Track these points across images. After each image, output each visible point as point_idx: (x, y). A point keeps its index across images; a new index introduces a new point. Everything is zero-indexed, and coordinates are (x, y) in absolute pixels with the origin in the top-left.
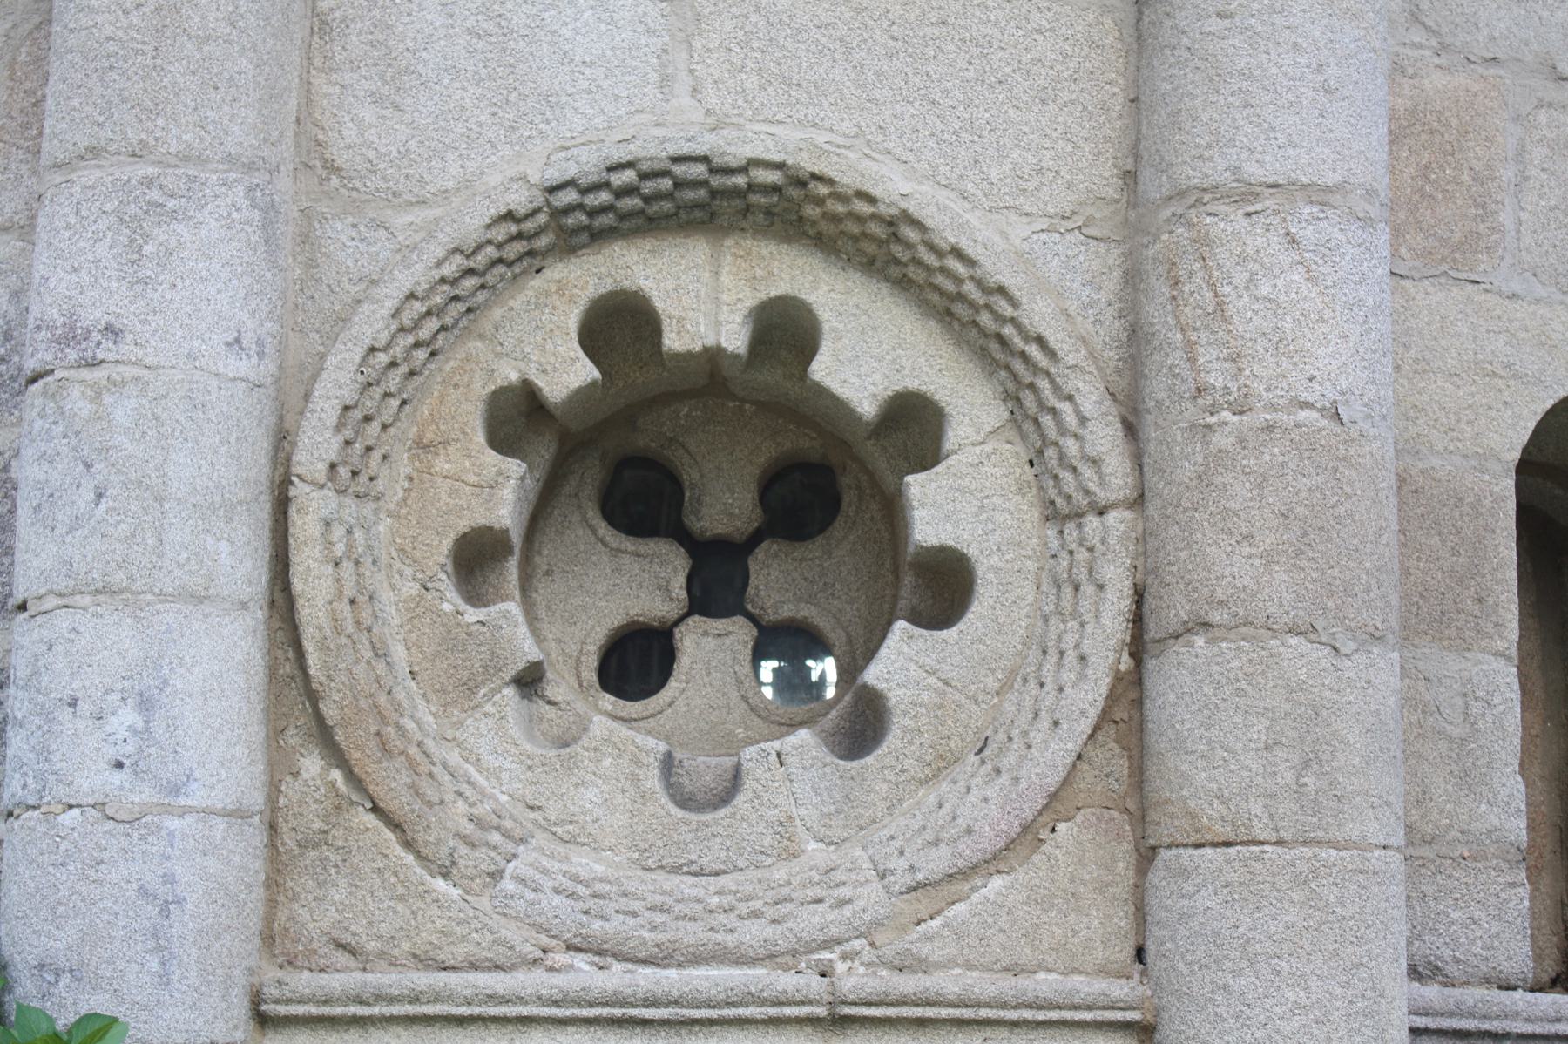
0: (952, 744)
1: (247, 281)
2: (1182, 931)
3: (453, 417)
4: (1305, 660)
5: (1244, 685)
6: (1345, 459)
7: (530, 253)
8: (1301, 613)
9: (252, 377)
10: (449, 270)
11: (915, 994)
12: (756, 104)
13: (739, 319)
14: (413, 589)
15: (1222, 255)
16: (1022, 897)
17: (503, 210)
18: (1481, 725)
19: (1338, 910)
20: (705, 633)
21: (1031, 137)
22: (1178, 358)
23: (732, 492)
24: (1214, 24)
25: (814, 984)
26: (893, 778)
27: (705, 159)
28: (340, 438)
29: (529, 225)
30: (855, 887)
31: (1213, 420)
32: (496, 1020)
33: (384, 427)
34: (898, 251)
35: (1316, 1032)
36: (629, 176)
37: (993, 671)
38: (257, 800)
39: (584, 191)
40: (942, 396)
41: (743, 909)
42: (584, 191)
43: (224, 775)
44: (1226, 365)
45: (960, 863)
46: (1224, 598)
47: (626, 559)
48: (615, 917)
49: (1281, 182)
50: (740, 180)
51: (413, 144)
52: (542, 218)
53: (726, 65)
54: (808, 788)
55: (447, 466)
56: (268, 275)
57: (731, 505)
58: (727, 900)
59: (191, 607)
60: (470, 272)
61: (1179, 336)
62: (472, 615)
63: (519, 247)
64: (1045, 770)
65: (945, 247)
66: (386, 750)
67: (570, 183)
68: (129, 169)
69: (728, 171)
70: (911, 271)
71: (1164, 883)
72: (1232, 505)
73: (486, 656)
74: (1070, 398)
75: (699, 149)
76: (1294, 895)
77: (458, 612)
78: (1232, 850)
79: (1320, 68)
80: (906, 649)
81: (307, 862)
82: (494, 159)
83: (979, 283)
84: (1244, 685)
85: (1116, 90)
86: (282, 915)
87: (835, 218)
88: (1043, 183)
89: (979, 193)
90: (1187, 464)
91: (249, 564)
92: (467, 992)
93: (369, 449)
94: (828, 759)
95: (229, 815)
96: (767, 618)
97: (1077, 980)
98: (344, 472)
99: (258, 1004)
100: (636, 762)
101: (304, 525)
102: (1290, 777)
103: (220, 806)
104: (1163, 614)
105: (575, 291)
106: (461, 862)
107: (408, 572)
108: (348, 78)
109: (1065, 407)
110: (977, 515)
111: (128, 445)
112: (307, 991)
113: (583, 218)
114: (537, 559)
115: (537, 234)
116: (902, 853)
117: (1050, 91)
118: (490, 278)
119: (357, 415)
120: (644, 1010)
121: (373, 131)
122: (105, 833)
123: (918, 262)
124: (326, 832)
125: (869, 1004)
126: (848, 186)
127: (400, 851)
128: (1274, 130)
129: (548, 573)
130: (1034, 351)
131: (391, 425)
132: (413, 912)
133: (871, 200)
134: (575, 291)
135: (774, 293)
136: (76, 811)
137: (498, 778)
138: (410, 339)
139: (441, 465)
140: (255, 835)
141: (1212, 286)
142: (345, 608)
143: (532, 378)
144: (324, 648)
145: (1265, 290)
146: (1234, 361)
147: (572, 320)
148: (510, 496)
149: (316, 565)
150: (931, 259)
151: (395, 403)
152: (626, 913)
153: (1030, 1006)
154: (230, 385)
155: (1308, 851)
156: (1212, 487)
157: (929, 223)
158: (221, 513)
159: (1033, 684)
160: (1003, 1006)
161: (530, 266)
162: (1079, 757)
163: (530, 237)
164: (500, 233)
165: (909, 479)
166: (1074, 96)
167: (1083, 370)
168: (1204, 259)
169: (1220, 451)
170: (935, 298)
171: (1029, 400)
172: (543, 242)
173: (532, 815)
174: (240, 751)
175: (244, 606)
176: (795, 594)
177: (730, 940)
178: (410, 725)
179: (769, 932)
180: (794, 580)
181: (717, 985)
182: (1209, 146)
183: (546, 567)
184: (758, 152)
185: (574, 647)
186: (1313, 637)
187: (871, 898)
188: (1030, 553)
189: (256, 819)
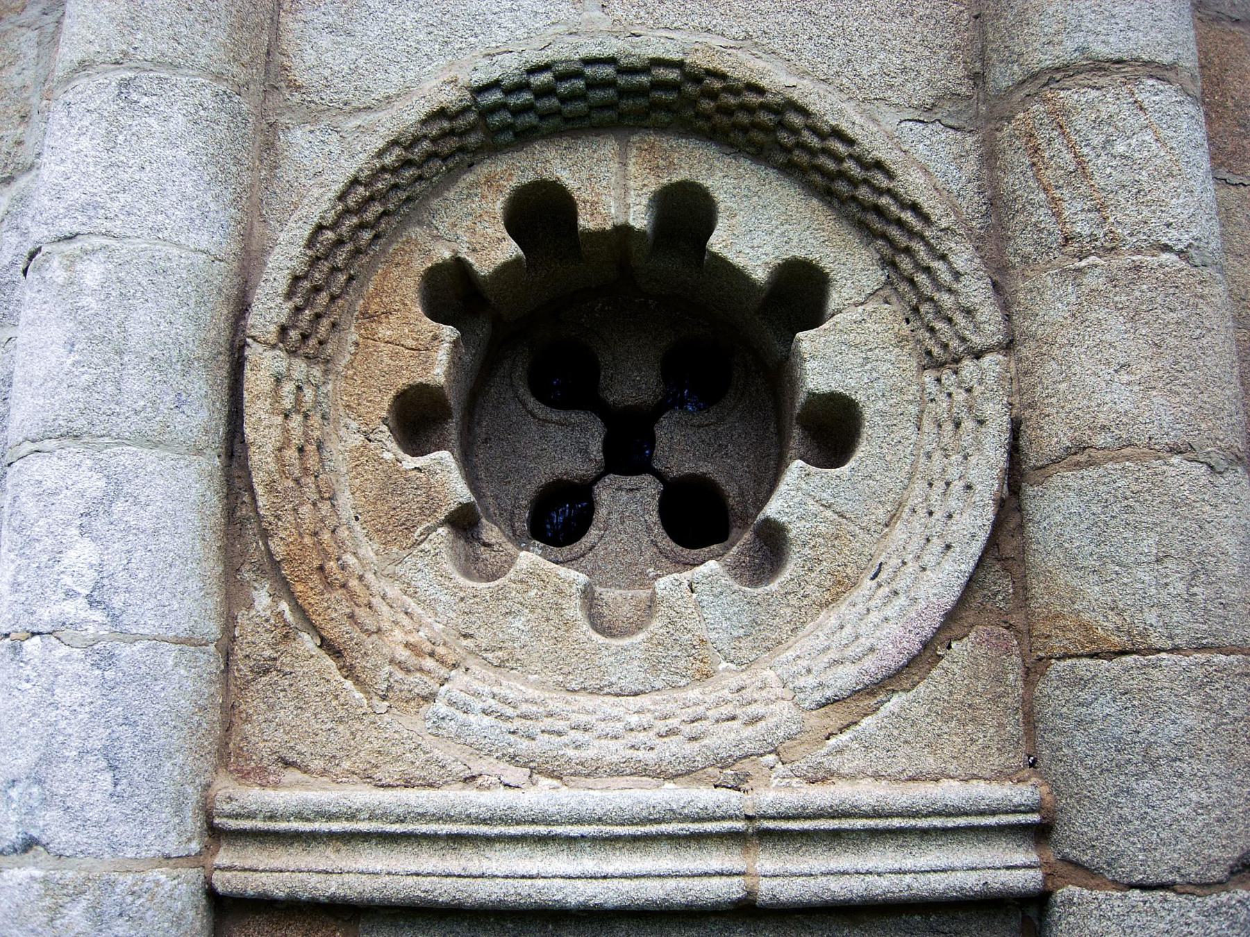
0: (849, 570)
2: (1079, 736)
3: (395, 291)
4: (1186, 478)
5: (1131, 502)
6: (1202, 297)
7: (462, 149)
8: (1179, 433)
9: (214, 251)
10: (389, 160)
11: (831, 807)
12: (656, 15)
13: (645, 201)
14: (359, 440)
15: (1080, 122)
16: (923, 710)
17: (436, 107)
19: (1231, 712)
20: (620, 489)
21: (894, 42)
22: (1043, 216)
23: (640, 370)
25: (733, 800)
26: (795, 602)
27: (611, 61)
28: (290, 305)
29: (461, 123)
30: (767, 704)
32: (425, 836)
33: (333, 298)
34: (784, 137)
35: (1218, 830)
36: (546, 77)
37: (883, 503)
38: (213, 629)
40: (827, 264)
41: (661, 726)
42: (509, 91)
43: (176, 606)
44: (1091, 215)
45: (867, 680)
46: (1106, 423)
47: (552, 428)
48: (540, 737)
49: (1125, 58)
50: (644, 79)
51: (362, 61)
52: (472, 117)
54: (718, 614)
55: (388, 333)
56: (234, 169)
57: (639, 381)
58: (646, 719)
59: (146, 451)
60: (407, 163)
61: (1042, 196)
62: (410, 462)
63: (453, 143)
64: (942, 590)
65: (826, 128)
66: (329, 585)
67: (495, 85)
68: (111, 75)
69: (632, 71)
71: (1058, 692)
72: (1107, 337)
73: (423, 499)
74: (943, 257)
75: (608, 52)
76: (1191, 699)
77: (397, 460)
78: (1129, 660)
80: (804, 486)
81: (259, 687)
82: (430, 68)
83: (859, 160)
85: (962, 8)
86: (235, 739)
87: (727, 111)
88: (907, 80)
89: (852, 86)
90: (1060, 305)
92: (400, 811)
93: (318, 316)
94: (736, 587)
95: (181, 643)
96: (671, 475)
98: (294, 334)
100: (559, 592)
101: (257, 381)
102: (1181, 587)
104: (1044, 442)
105: (501, 182)
106: (397, 686)
107: (354, 425)
108: (311, 15)
109: (937, 265)
110: (862, 365)
111: (93, 305)
112: (254, 807)
113: (507, 117)
114: (477, 430)
116: (809, 671)
117: (907, 7)
119: (306, 284)
120: (569, 827)
121: (329, 54)
122: (61, 659)
123: (803, 146)
124: (275, 659)
125: (788, 818)
126: (738, 80)
128: (1114, 16)
129: (486, 441)
130: (907, 216)
131: (339, 297)
132: (352, 733)
133: (760, 91)
134: (501, 182)
135: (675, 179)
136: (37, 639)
137: (434, 609)
139: (384, 332)
140: (209, 661)
141: (1072, 148)
142: (291, 454)
143: (463, 256)
144: (271, 488)
145: (1121, 148)
146: (1098, 210)
147: (498, 205)
148: (444, 357)
149: (267, 416)
150: (814, 141)
151: (342, 278)
152: (550, 733)
153: (938, 814)
154: (192, 255)
155: (1201, 657)
156: (1087, 323)
157: (812, 108)
158: (179, 367)
159: (922, 513)
160: (916, 814)
161: (462, 160)
162: (971, 579)
163: (463, 134)
164: (434, 130)
165: (800, 335)
166: (928, 12)
167: (954, 233)
168: (1061, 127)
169: (1092, 290)
170: (817, 178)
171: (905, 263)
172: (473, 139)
173: (465, 642)
174: (193, 584)
175: (200, 452)
176: (694, 455)
177: (650, 757)
178: (349, 559)
179: (691, 748)
180: (693, 443)
181: (640, 802)
182: (1058, 33)
183: (484, 436)
184: (660, 53)
185: (509, 502)
186: (1192, 456)
187: (781, 715)
188: (911, 398)
189: (212, 648)
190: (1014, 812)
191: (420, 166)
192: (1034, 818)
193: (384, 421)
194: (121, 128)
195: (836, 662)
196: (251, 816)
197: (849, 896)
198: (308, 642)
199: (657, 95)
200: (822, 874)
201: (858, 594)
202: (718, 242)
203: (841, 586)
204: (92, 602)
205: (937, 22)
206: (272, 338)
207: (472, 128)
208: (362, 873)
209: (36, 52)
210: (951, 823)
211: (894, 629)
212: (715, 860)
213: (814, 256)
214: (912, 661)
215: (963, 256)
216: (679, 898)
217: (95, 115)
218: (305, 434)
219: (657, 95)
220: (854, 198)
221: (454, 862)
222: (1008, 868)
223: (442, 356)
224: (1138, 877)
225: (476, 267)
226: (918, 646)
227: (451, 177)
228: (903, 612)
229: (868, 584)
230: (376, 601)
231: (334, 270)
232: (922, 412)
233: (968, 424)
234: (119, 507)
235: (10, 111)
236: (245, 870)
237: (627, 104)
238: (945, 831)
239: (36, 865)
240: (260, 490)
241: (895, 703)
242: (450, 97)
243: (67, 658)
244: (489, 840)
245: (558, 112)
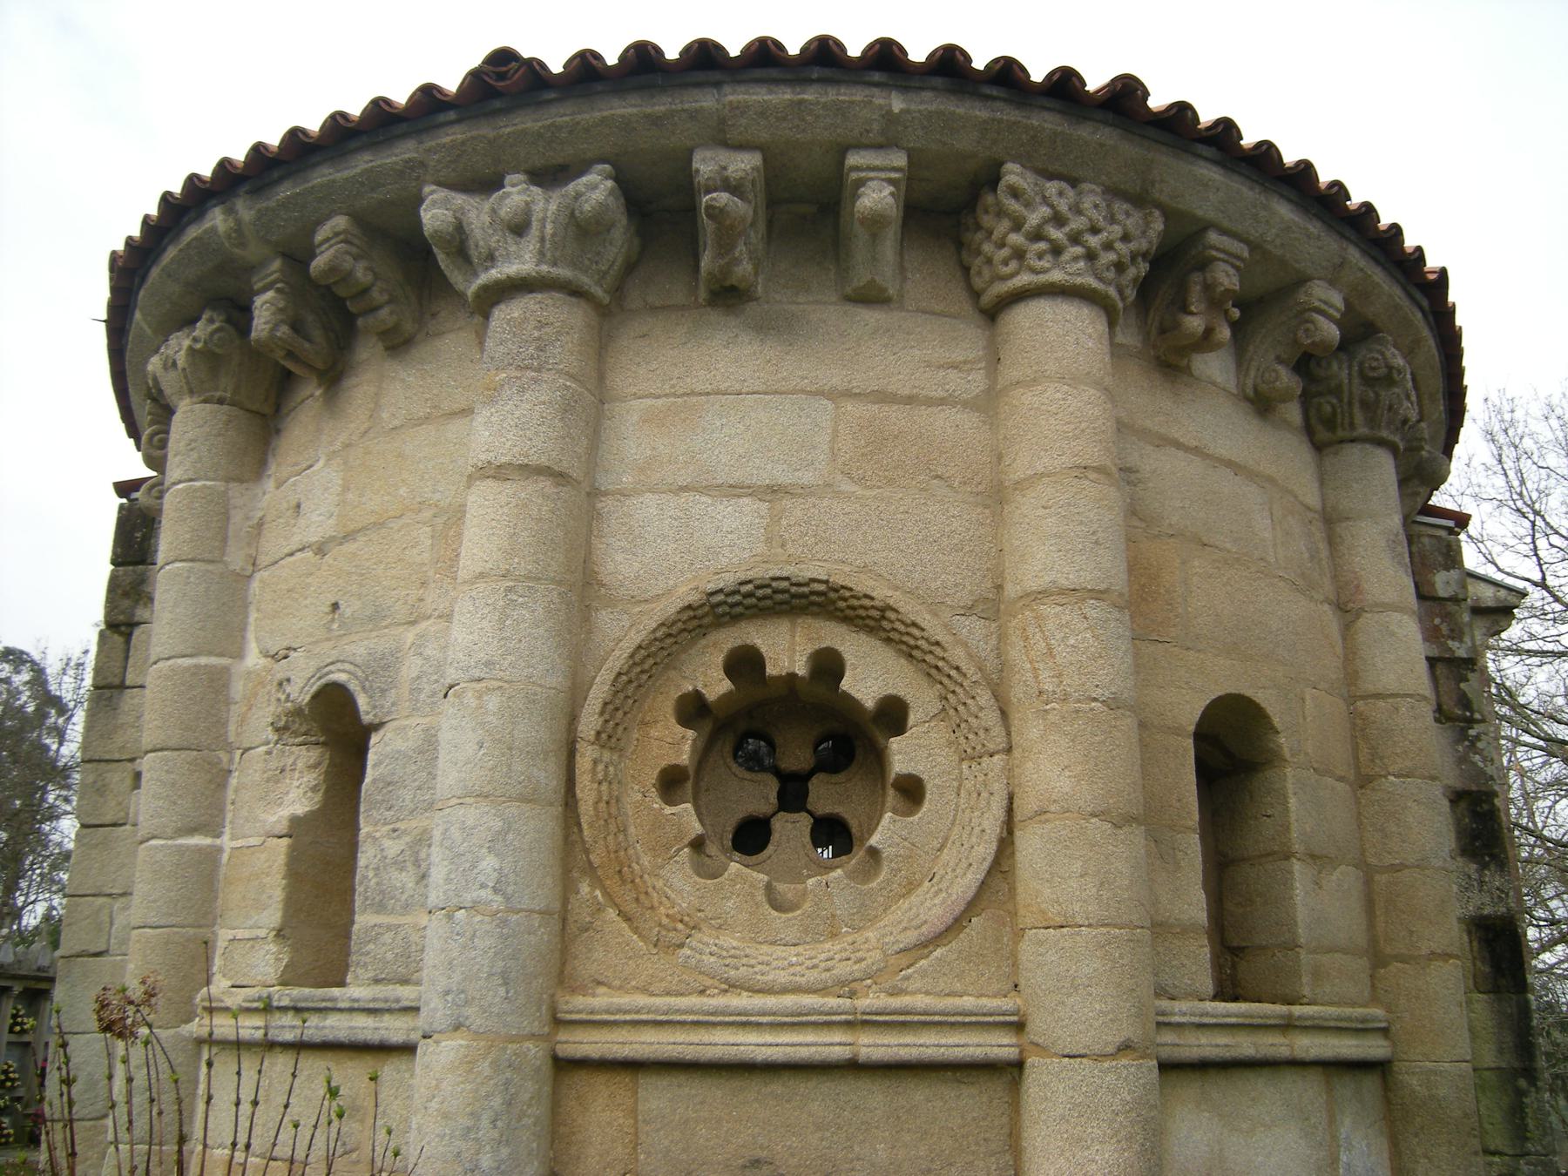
1: (557, 639)
5: (1068, 843)
7: (700, 626)
10: (659, 634)
17: (686, 604)
18: (1182, 864)
20: (787, 821)
24: (1041, 512)
27: (787, 579)
28: (602, 719)
29: (700, 612)
31: (1048, 707)
32: (679, 1022)
33: (625, 713)
34: (885, 624)
36: (749, 587)
37: (937, 838)
38: (557, 905)
39: (727, 595)
40: (909, 699)
41: (809, 963)
42: (727, 595)
45: (923, 938)
50: (806, 589)
51: (642, 572)
52: (706, 609)
53: (799, 533)
58: (801, 959)
60: (670, 635)
61: (1029, 666)
62: (668, 810)
63: (696, 623)
65: (909, 622)
66: (624, 882)
69: (799, 585)
70: (892, 635)
74: (973, 698)
75: (785, 574)
78: (1065, 930)
79: (1094, 533)
84: (1068, 843)
86: (568, 969)
87: (853, 608)
91: (555, 782)
93: (617, 724)
97: (984, 1001)
98: (604, 736)
99: (556, 1014)
101: (584, 762)
102: (1094, 890)
103: (538, 908)
107: (636, 787)
109: (969, 701)
112: (581, 1007)
113: (727, 609)
115: (703, 617)
116: (891, 934)
118: (679, 639)
119: (611, 707)
124: (592, 923)
125: (877, 1014)
127: (628, 932)
129: (706, 791)
130: (953, 673)
133: (872, 598)
136: (463, 911)
138: (639, 669)
139: (654, 733)
141: (1045, 639)
142: (602, 805)
143: (700, 689)
144: (591, 825)
145: (1072, 641)
147: (720, 659)
150: (902, 628)
151: (630, 701)
155: (1104, 930)
157: (900, 610)
159: (958, 844)
160: (947, 1014)
162: (983, 882)
163: (700, 618)
164: (685, 617)
165: (892, 739)
170: (904, 648)
172: (706, 621)
174: (549, 880)
175: (551, 804)
178: (636, 867)
184: (815, 576)
186: (1103, 818)
189: (556, 916)
190: (1003, 1015)
191: (676, 637)
192: (1015, 1018)
193: (654, 786)
194: (507, 617)
195: (905, 929)
196: (579, 1012)
197: (910, 1058)
198: (611, 913)
199: (814, 598)
200: (896, 1046)
201: (920, 891)
202: (846, 685)
203: (911, 887)
204: (495, 890)
205: (977, 555)
206: (592, 738)
207: (706, 615)
208: (643, 1043)
209: (430, 541)
210: (967, 1019)
211: (938, 911)
212: (838, 1037)
213: (901, 694)
214: (948, 929)
215: (984, 697)
216: (817, 1057)
217: (491, 607)
218: (610, 793)
219: (814, 598)
220: (924, 661)
221: (694, 1036)
222: (999, 1046)
223: (687, 747)
224: (1067, 1051)
225: (707, 696)
226: (951, 920)
227: (693, 642)
228: (944, 901)
229: (927, 884)
230: (650, 890)
231: (627, 697)
232: (960, 785)
233: (985, 795)
234: (510, 836)
235: (414, 578)
236: (575, 1043)
237: (796, 602)
238: (964, 1024)
239: (462, 1039)
240: (585, 826)
241: (938, 952)
242: (694, 598)
243: (481, 922)
244: (714, 1024)
245: (756, 606)
